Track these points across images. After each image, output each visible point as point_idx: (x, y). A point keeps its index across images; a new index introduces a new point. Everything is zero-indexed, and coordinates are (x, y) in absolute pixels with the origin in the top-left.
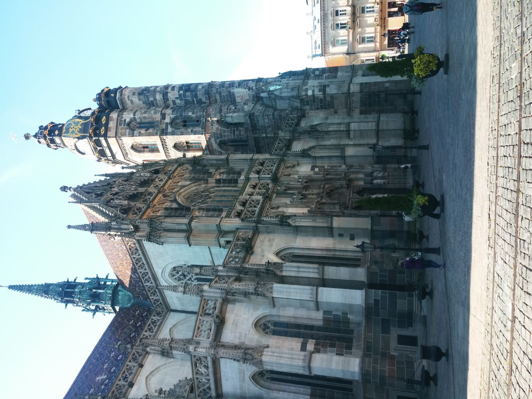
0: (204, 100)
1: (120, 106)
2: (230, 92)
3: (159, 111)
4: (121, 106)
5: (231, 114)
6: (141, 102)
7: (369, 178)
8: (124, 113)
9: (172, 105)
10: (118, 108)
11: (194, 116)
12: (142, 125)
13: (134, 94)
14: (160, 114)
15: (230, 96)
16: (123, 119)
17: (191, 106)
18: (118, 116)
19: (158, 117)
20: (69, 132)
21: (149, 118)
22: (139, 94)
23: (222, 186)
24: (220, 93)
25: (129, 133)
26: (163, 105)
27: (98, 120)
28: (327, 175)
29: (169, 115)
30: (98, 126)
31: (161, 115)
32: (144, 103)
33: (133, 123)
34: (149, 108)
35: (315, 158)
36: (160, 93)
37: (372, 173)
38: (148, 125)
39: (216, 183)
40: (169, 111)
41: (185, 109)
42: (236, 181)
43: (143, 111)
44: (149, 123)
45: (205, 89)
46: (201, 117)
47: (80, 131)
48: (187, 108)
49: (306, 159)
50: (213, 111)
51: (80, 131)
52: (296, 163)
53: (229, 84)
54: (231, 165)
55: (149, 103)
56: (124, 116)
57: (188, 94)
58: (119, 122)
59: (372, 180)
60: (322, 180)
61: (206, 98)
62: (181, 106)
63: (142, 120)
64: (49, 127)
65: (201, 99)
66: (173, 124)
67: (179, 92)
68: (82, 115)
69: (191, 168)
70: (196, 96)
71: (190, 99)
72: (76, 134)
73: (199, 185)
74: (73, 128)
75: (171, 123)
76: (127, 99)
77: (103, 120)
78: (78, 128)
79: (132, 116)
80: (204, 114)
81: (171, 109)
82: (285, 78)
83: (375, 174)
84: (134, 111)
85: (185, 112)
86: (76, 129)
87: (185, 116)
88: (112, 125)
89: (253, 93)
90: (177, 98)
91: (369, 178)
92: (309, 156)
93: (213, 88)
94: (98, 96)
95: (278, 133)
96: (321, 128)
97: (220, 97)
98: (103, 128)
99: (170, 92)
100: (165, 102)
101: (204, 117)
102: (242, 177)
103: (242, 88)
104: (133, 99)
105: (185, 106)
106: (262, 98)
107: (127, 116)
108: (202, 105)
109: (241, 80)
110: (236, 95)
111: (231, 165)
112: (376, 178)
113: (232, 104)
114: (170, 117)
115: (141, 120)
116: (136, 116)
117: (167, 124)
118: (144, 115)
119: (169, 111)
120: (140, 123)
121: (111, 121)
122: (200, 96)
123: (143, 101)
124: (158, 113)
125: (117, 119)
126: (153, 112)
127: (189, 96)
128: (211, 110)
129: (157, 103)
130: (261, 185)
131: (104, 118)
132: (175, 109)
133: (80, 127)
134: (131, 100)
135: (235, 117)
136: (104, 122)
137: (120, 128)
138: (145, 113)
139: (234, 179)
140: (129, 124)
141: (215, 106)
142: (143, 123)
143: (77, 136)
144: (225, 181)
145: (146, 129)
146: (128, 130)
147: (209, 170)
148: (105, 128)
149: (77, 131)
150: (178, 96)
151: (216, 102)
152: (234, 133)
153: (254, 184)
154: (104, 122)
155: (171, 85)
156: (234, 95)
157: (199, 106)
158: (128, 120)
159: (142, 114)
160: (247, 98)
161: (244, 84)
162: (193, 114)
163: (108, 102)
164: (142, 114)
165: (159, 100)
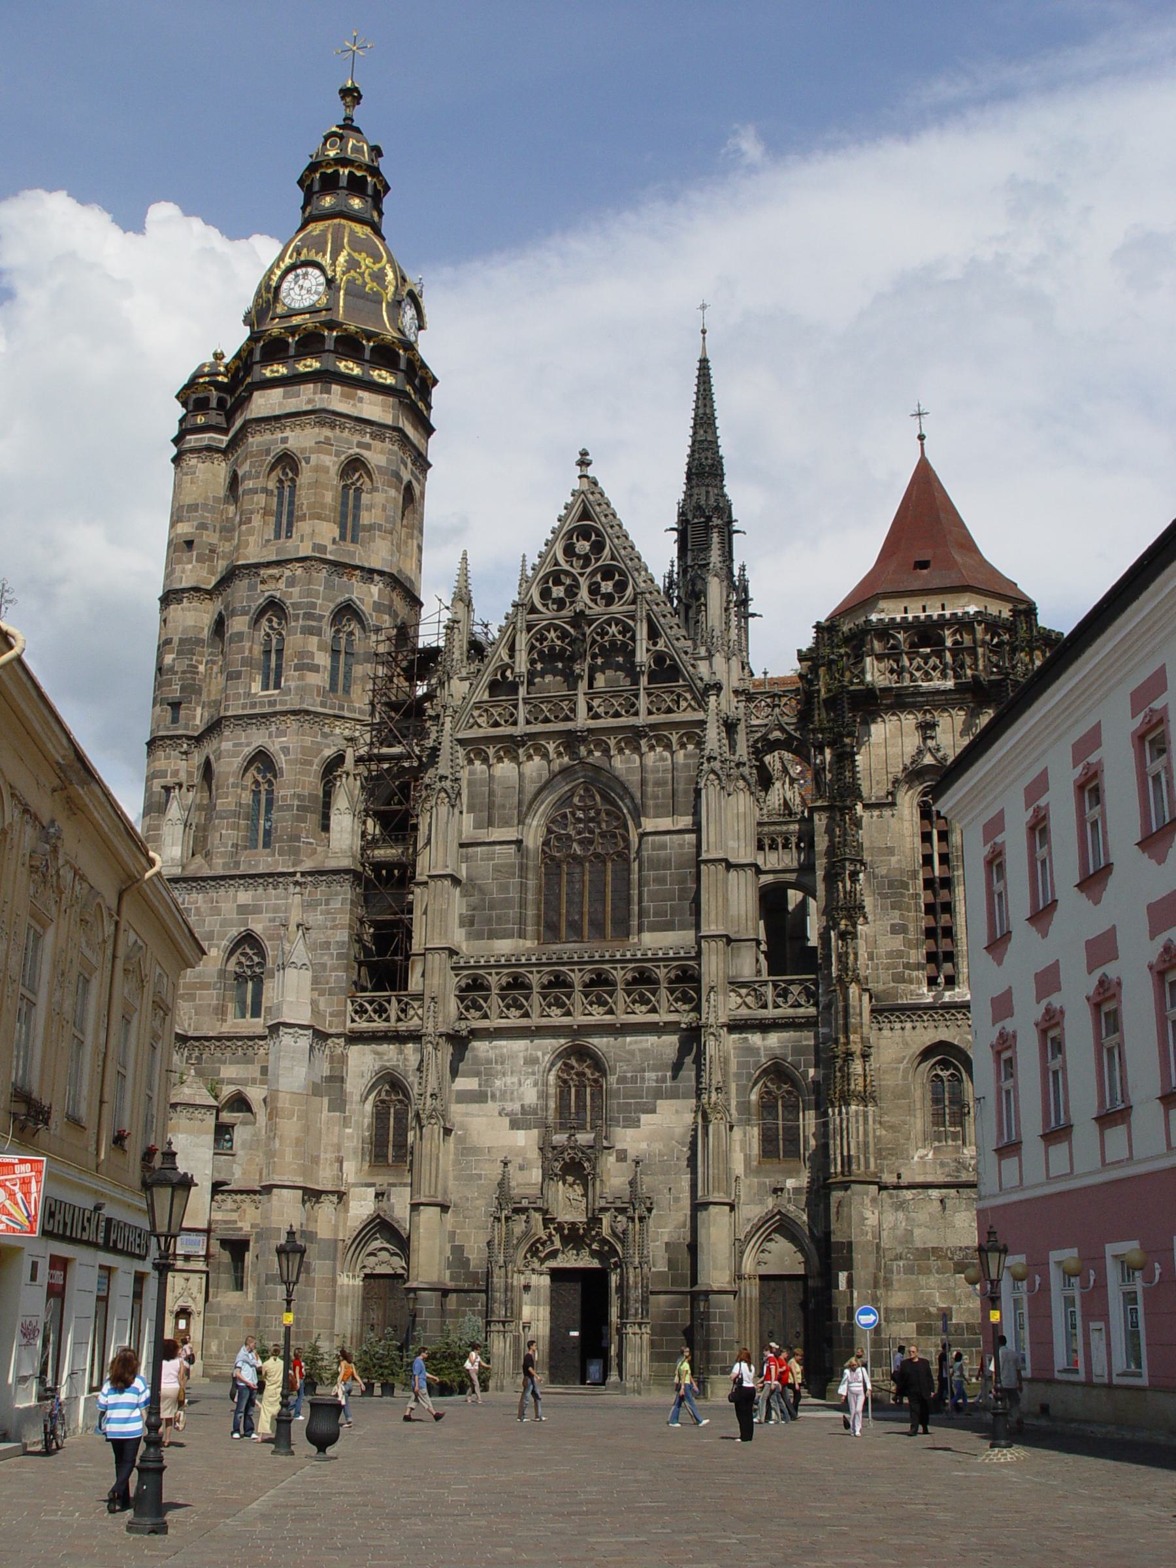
30: (367, 356)
78: (365, 284)
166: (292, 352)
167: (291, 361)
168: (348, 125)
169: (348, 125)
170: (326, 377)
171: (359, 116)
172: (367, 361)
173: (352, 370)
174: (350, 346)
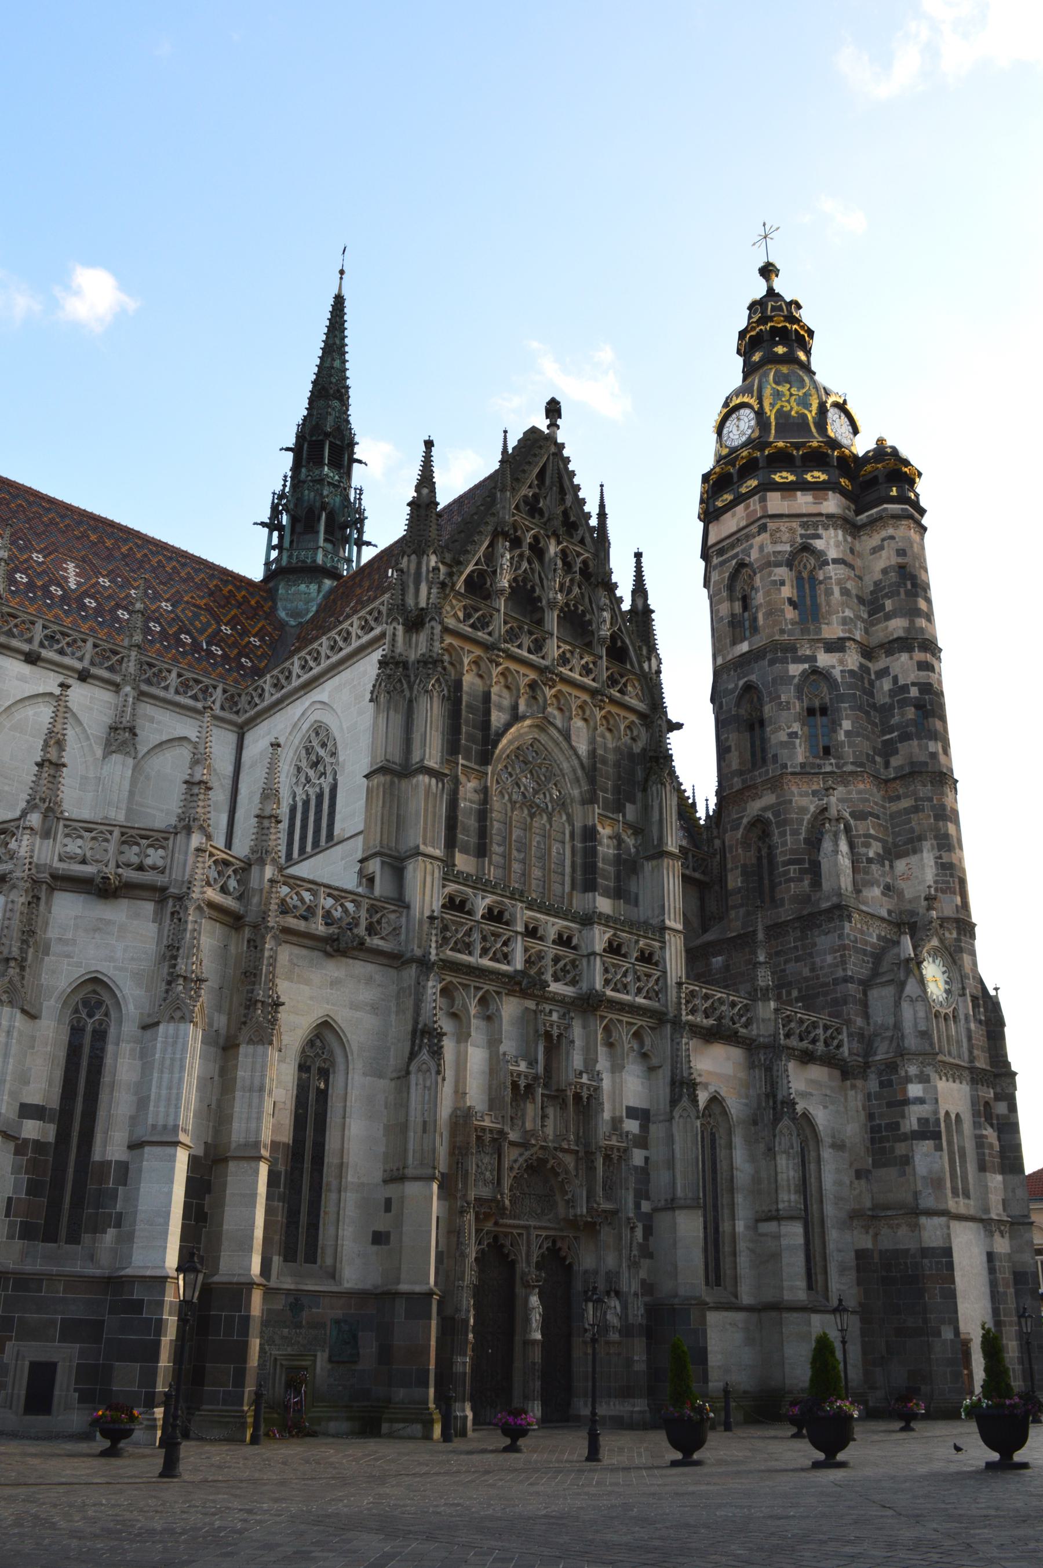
0: (895, 761)
1: (863, 517)
2: (921, 838)
3: (850, 631)
4: (865, 520)
5: (844, 847)
6: (877, 576)
8: (840, 532)
9: (874, 667)
10: (858, 512)
11: (842, 737)
12: (807, 586)
13: (901, 552)
14: (842, 635)
15: (911, 841)
16: (820, 531)
17: (875, 724)
18: (829, 516)
19: (833, 630)
21: (828, 604)
22: (902, 568)
23: (573, 848)
24: (916, 809)
25: (779, 552)
26: (874, 641)
27: (817, 459)
28: (607, 1158)
29: (841, 662)
30: (798, 462)
31: (839, 639)
32: (876, 584)
33: (812, 561)
34: (861, 600)
35: (671, 1119)
36: (907, 630)
38: (808, 602)
39: (585, 827)
40: (852, 660)
41: (860, 708)
42: (590, 885)
43: (849, 585)
44: (816, 605)
45: (926, 764)
46: (838, 757)
47: (781, 414)
48: (867, 713)
49: (668, 1090)
50: (859, 792)
51: (781, 414)
52: (655, 1061)
53: (947, 836)
54: (648, 866)
55: (876, 599)
56: (832, 531)
57: (911, 713)
58: (812, 521)
60: (587, 1145)
61: (901, 767)
62: (872, 695)
63: (822, 586)
64: (795, 327)
65: (896, 752)
66: (813, 677)
68: (833, 414)
69: (637, 748)
70: (905, 737)
71: (896, 720)
72: (772, 405)
73: (577, 780)
74: (791, 395)
75: (815, 671)
76: (884, 534)
77: (816, 474)
78: (792, 408)
79: (832, 554)
80: (849, 768)
81: (861, 666)
82: (976, 1006)
84: (849, 558)
85: (851, 708)
86: (788, 401)
87: (838, 710)
88: (803, 502)
89: (922, 911)
90: (895, 679)
92: (674, 1102)
93: (933, 785)
94: (889, 450)
95: (769, 1000)
96: (785, 1131)
97: (907, 811)
98: (791, 478)
99: (911, 658)
100: (881, 646)
101: (838, 766)
102: (604, 905)
103: (937, 875)
104: (884, 553)
105: (874, 706)
106: (897, 943)
107: (832, 542)
108: (878, 759)
109: (963, 871)
110: (913, 859)
111: (648, 866)
113: (884, 848)
114: (833, 667)
115: (821, 582)
116: (831, 567)
117: (813, 659)
118: (836, 591)
119: (852, 660)
120: (813, 579)
121: (815, 498)
122: (903, 748)
123: (880, 581)
124: (843, 631)
125: (820, 515)
126: (848, 613)
127: (902, 715)
128: (861, 786)
129: (878, 621)
130: (573, 962)
131: (823, 477)
132: (862, 678)
133: (793, 413)
134: (881, 548)
135: (836, 863)
136: (809, 477)
137: (794, 525)
138: (845, 592)
139: (595, 878)
140: (806, 548)
141: (877, 796)
142: (813, 589)
143: (767, 408)
144: (590, 853)
145: (795, 599)
146: (787, 548)
147: (634, 802)
148: (792, 482)
149: (782, 407)
150: (901, 682)
151: (891, 800)
153: (575, 941)
154: (809, 477)
155: (939, 659)
156: (915, 852)
157: (874, 749)
158: (819, 544)
159: (839, 582)
160: (908, 894)
161: (948, 882)
162: (848, 733)
163: (872, 482)
164: (839, 582)
165: (887, 627)
166: (735, 479)
167: (735, 486)
168: (771, 293)
169: (771, 293)
171: (778, 285)
172: (799, 467)
173: (787, 478)
174: (782, 460)
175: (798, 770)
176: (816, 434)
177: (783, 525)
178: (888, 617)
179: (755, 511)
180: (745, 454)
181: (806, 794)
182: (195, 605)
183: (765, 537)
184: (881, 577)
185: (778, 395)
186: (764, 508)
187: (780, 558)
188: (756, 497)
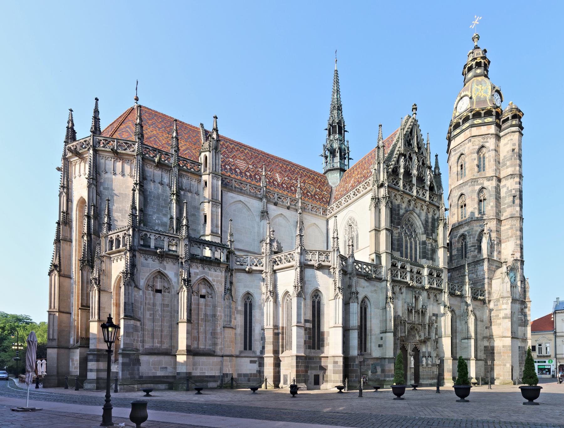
7: (427, 355)
20: (477, 85)
29: (491, 184)
37: (431, 357)
47: (478, 97)
51: (478, 97)
59: (425, 357)
61: (507, 216)
67: (513, 189)
74: (482, 89)
83: (430, 359)
90: (508, 188)
91: (427, 355)
112: (427, 360)
114: (489, 186)
117: (483, 183)
123: (506, 155)
133: (482, 97)
149: (478, 94)
152: (472, 246)
170: (472, 126)
175: (476, 219)
176: (489, 104)
177: (476, 139)
178: (507, 168)
179: (467, 135)
180: (465, 114)
181: (478, 226)
182: (309, 184)
183: (470, 143)
184: (506, 154)
185: (478, 89)
186: (471, 134)
187: (474, 151)
188: (468, 130)
